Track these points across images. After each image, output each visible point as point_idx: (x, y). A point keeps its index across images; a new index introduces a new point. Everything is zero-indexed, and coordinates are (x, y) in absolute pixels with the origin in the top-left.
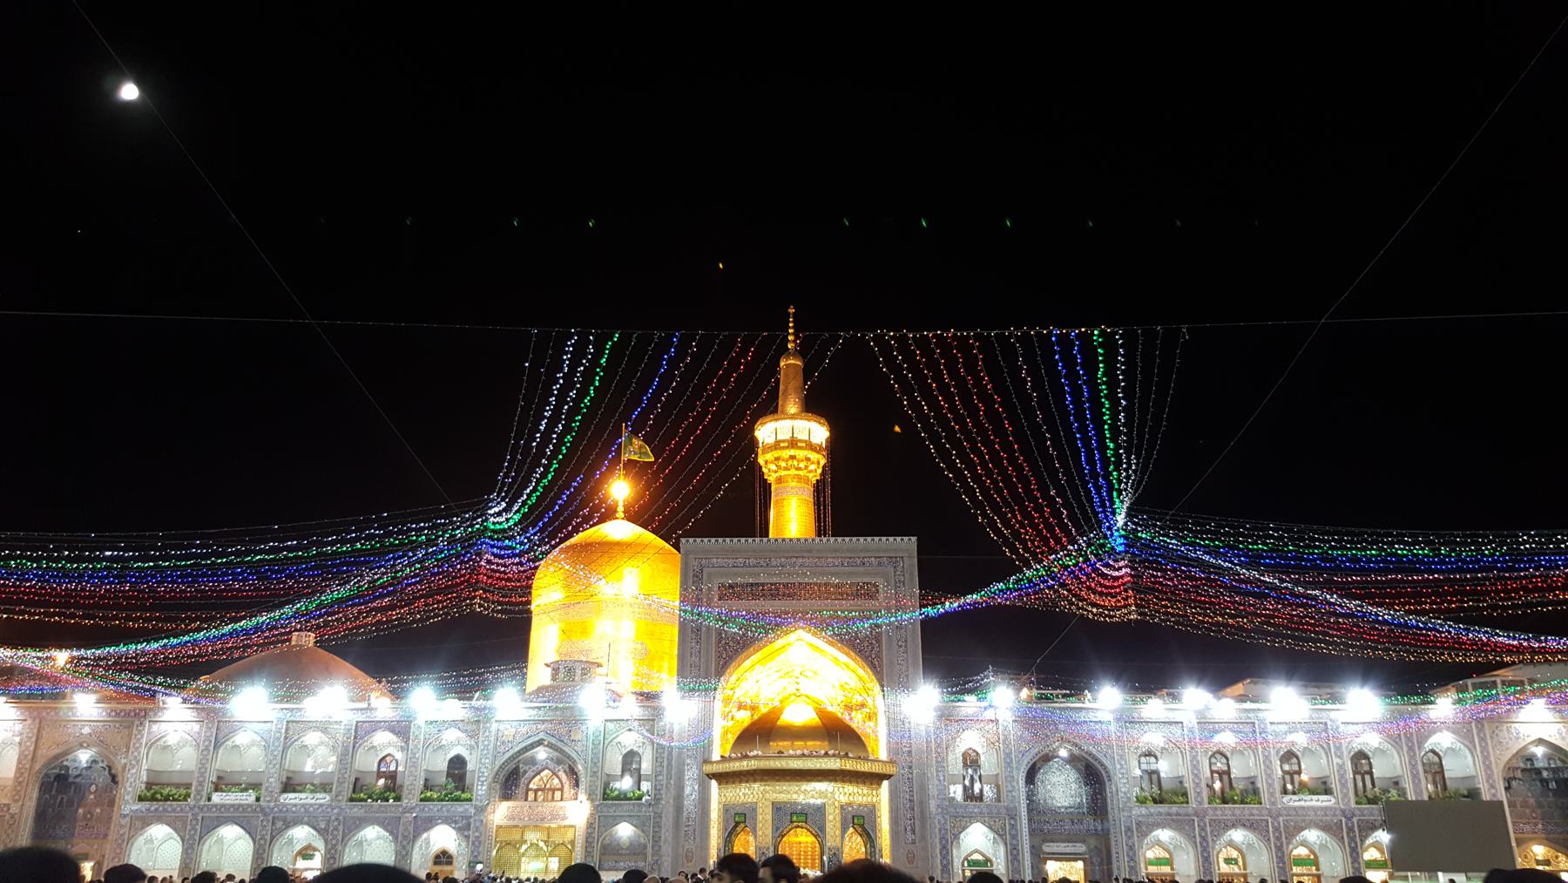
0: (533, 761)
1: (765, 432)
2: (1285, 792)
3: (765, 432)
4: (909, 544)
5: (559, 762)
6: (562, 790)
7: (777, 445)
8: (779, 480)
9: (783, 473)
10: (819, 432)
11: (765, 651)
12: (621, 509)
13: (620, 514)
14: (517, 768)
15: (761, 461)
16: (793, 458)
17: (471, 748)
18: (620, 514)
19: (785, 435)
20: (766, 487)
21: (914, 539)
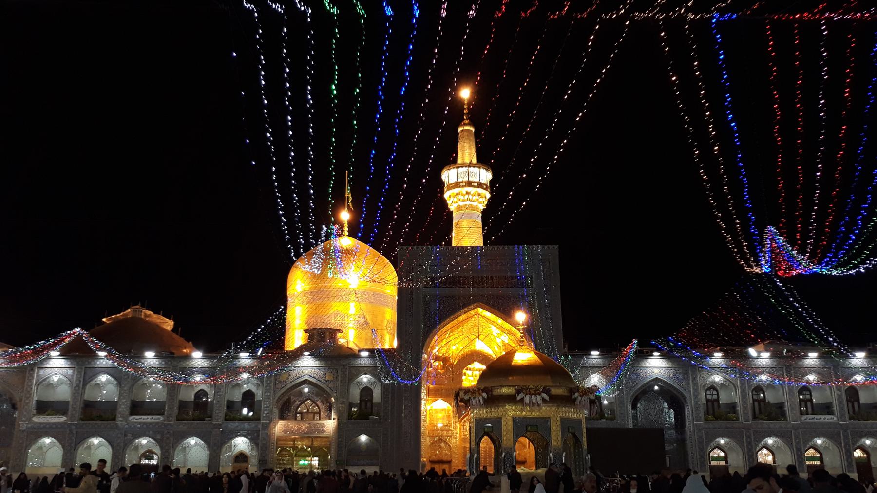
0: (301, 393)
1: (449, 176)
2: (802, 413)
3: (449, 176)
4: (554, 250)
5: (317, 395)
6: (319, 413)
7: (457, 185)
8: (459, 209)
9: (461, 204)
10: (486, 176)
11: (455, 321)
12: (346, 229)
14: (289, 399)
15: (446, 196)
16: (468, 193)
17: (258, 385)
19: (464, 178)
20: (450, 214)
21: (556, 247)
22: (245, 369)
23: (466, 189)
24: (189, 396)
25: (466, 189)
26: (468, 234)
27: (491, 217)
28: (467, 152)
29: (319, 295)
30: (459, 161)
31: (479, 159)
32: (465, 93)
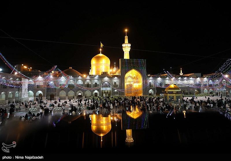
1: (123, 45)
3: (123, 45)
8: (125, 51)
10: (130, 45)
12: (101, 52)
13: (101, 53)
18: (101, 53)
22: (96, 79)
23: (127, 48)
24: (86, 83)
25: (127, 48)
26: (127, 56)
27: (131, 53)
28: (126, 41)
29: (97, 65)
30: (125, 43)
31: (128, 43)
32: (126, 30)
